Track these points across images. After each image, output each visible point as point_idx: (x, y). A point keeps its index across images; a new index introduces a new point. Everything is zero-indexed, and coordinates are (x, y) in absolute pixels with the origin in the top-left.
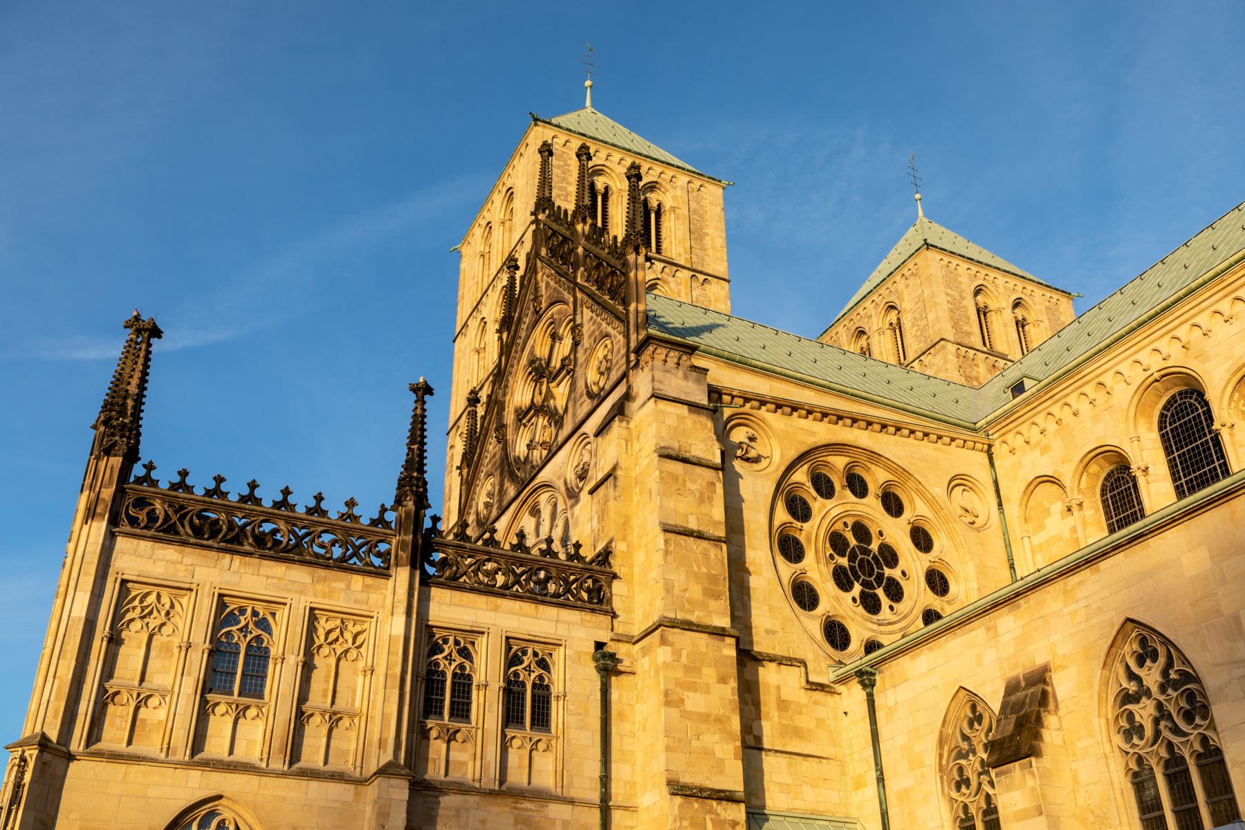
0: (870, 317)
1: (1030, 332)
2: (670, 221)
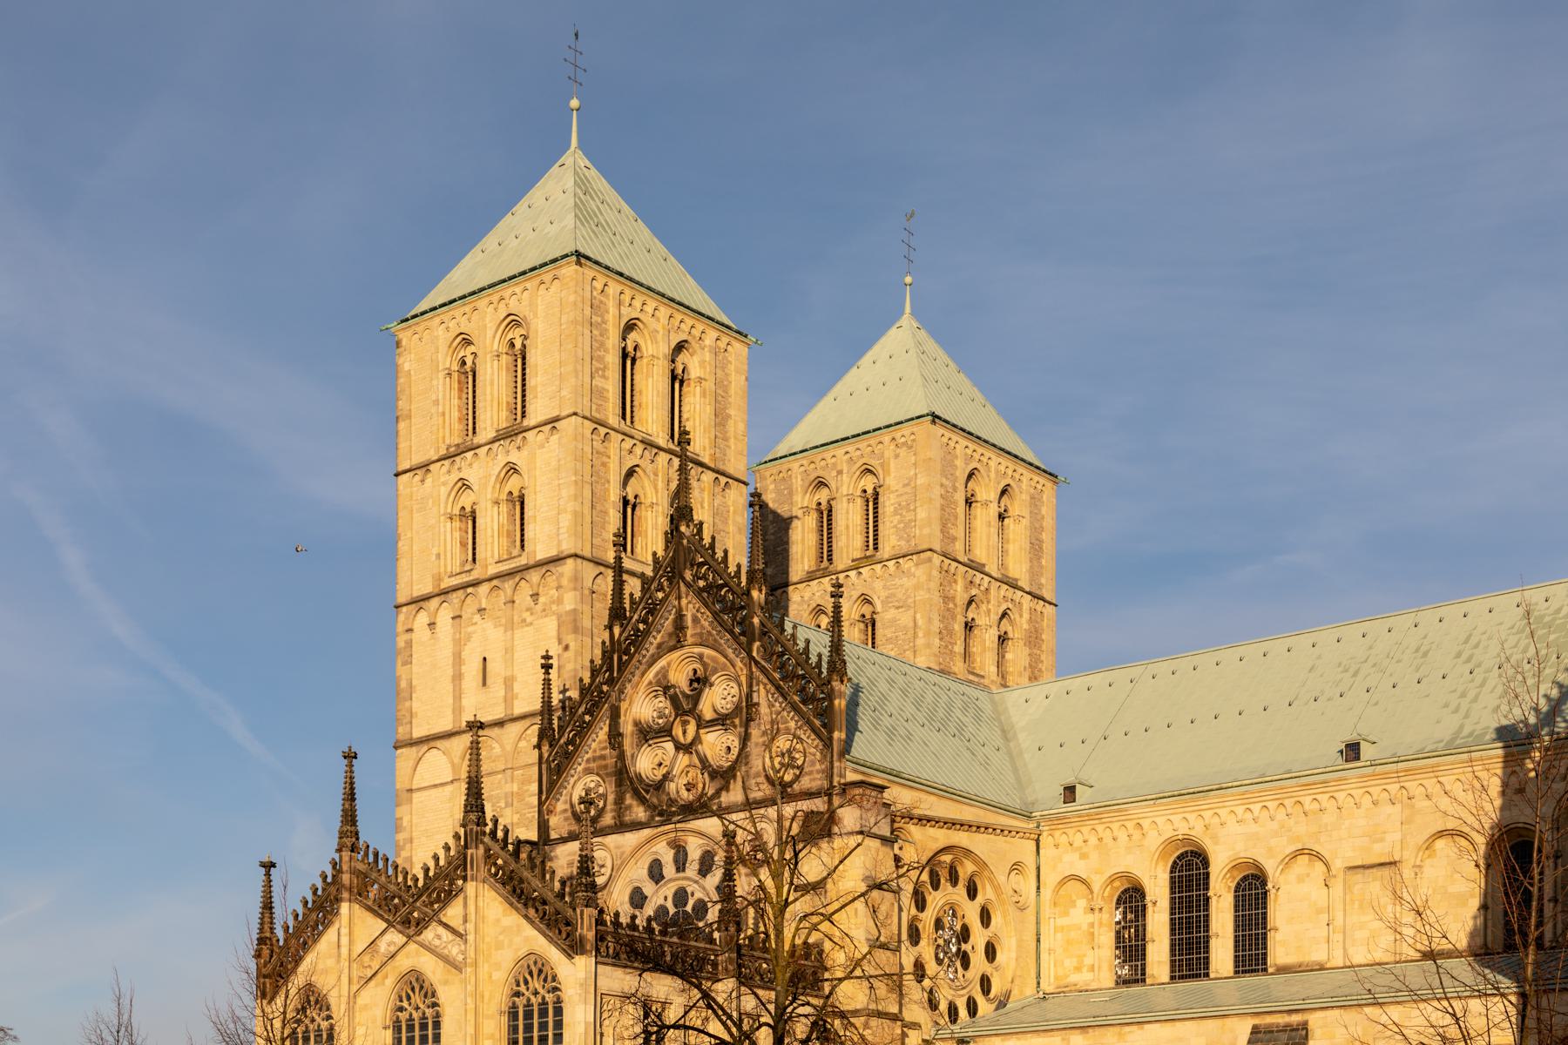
0: (840, 472)
1: (1009, 528)
2: (694, 395)
